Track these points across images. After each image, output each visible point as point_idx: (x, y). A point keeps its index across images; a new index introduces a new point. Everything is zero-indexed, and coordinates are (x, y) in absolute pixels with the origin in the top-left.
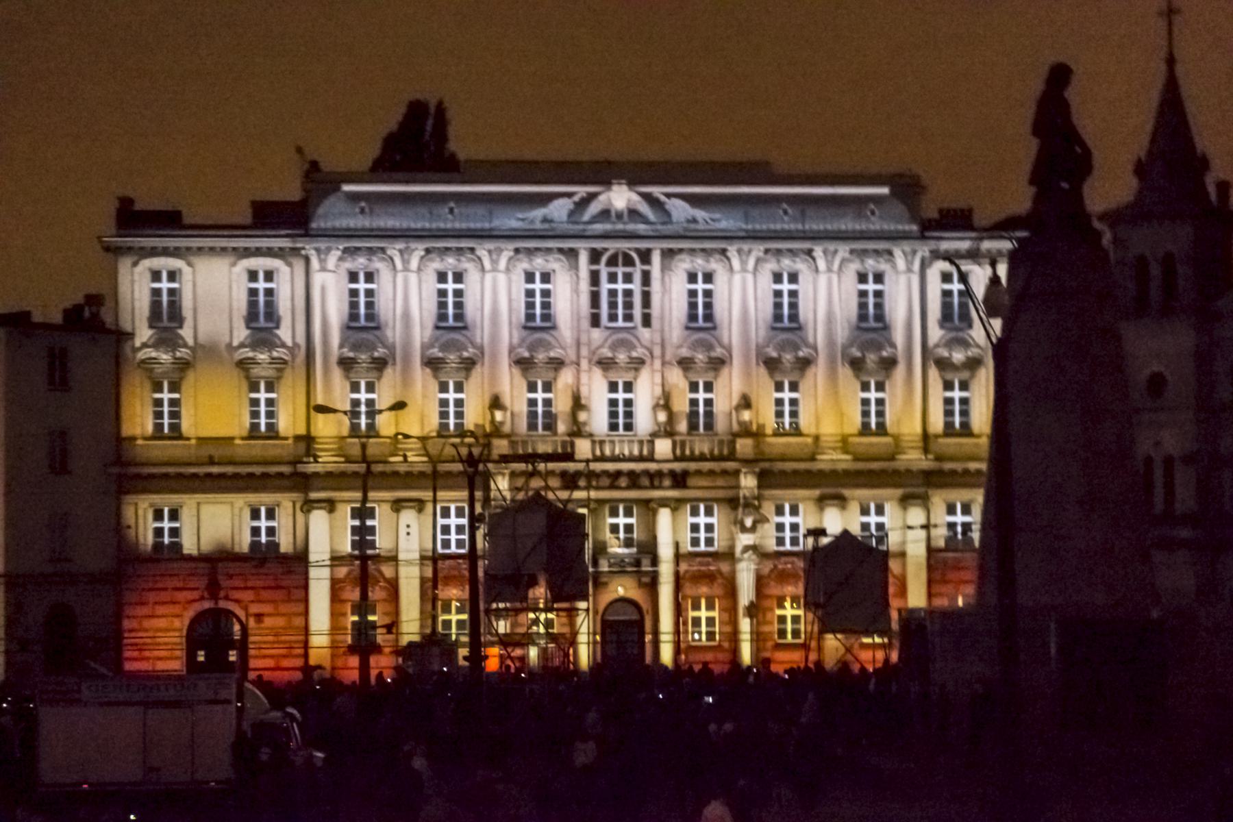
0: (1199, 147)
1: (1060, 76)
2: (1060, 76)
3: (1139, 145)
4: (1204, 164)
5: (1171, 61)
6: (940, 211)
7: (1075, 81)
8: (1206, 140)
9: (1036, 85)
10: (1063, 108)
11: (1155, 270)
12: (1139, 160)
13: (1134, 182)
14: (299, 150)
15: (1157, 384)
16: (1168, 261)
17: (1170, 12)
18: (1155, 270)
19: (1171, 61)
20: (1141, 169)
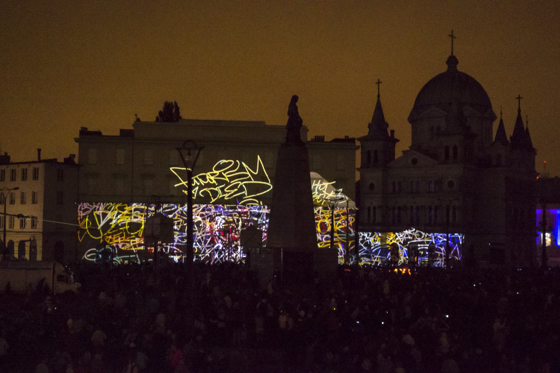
0: (386, 120)
1: (295, 99)
2: (295, 99)
3: (370, 120)
4: (387, 125)
5: (379, 96)
6: (315, 137)
7: (299, 100)
8: (387, 119)
9: (289, 101)
10: (296, 108)
11: (372, 155)
12: (369, 124)
13: (367, 130)
14: (136, 115)
15: (372, 186)
16: (376, 152)
17: (379, 83)
18: (372, 155)
19: (379, 96)
20: (370, 126)
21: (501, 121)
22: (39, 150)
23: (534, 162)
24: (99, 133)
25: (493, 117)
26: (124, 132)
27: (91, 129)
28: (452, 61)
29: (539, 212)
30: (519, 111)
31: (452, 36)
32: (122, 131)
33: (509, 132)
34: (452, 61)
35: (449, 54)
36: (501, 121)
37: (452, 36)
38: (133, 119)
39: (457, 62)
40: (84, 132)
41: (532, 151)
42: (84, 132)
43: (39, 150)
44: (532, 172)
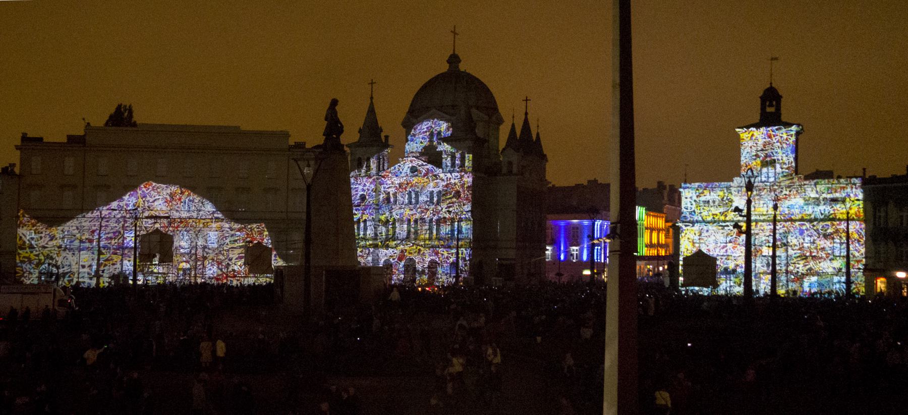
22: (864, 169)
23: (545, 169)
24: (40, 140)
25: (500, 121)
26: (72, 139)
27: (30, 135)
28: (454, 60)
29: (549, 223)
30: (526, 114)
31: (455, 33)
32: (70, 138)
34: (454, 60)
35: (452, 52)
36: (513, 125)
37: (455, 33)
38: (83, 124)
39: (460, 61)
40: (25, 138)
42: (25, 138)
43: (864, 169)
44: (542, 180)
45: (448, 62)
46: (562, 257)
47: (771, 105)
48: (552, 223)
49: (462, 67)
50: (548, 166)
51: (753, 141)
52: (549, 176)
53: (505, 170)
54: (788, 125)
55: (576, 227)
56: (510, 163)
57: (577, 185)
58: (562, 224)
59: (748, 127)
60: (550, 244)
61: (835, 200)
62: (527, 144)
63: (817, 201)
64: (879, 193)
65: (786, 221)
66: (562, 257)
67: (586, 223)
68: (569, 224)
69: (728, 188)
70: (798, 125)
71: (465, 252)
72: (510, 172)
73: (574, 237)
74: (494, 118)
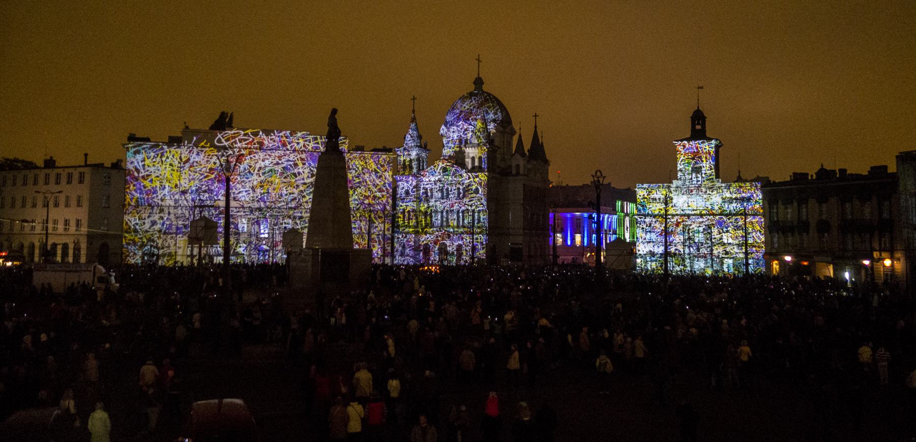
1: (334, 112)
2: (334, 112)
21: (520, 136)
25: (513, 132)
28: (479, 82)
31: (479, 61)
33: (527, 146)
34: (479, 82)
36: (520, 136)
37: (479, 61)
41: (546, 162)
44: (546, 181)
45: (475, 83)
46: (569, 243)
47: (698, 124)
48: (556, 215)
49: (485, 88)
50: (550, 168)
51: (683, 150)
52: (550, 178)
53: (514, 172)
54: (710, 139)
55: (578, 219)
56: (518, 166)
57: (584, 185)
58: (569, 216)
59: (682, 141)
60: (559, 232)
61: (742, 200)
62: (537, 152)
63: (731, 201)
64: (774, 193)
65: (710, 215)
66: (569, 243)
67: (586, 215)
68: (573, 217)
69: (669, 187)
70: (716, 140)
71: (482, 238)
72: (518, 174)
73: (577, 228)
74: (508, 130)
